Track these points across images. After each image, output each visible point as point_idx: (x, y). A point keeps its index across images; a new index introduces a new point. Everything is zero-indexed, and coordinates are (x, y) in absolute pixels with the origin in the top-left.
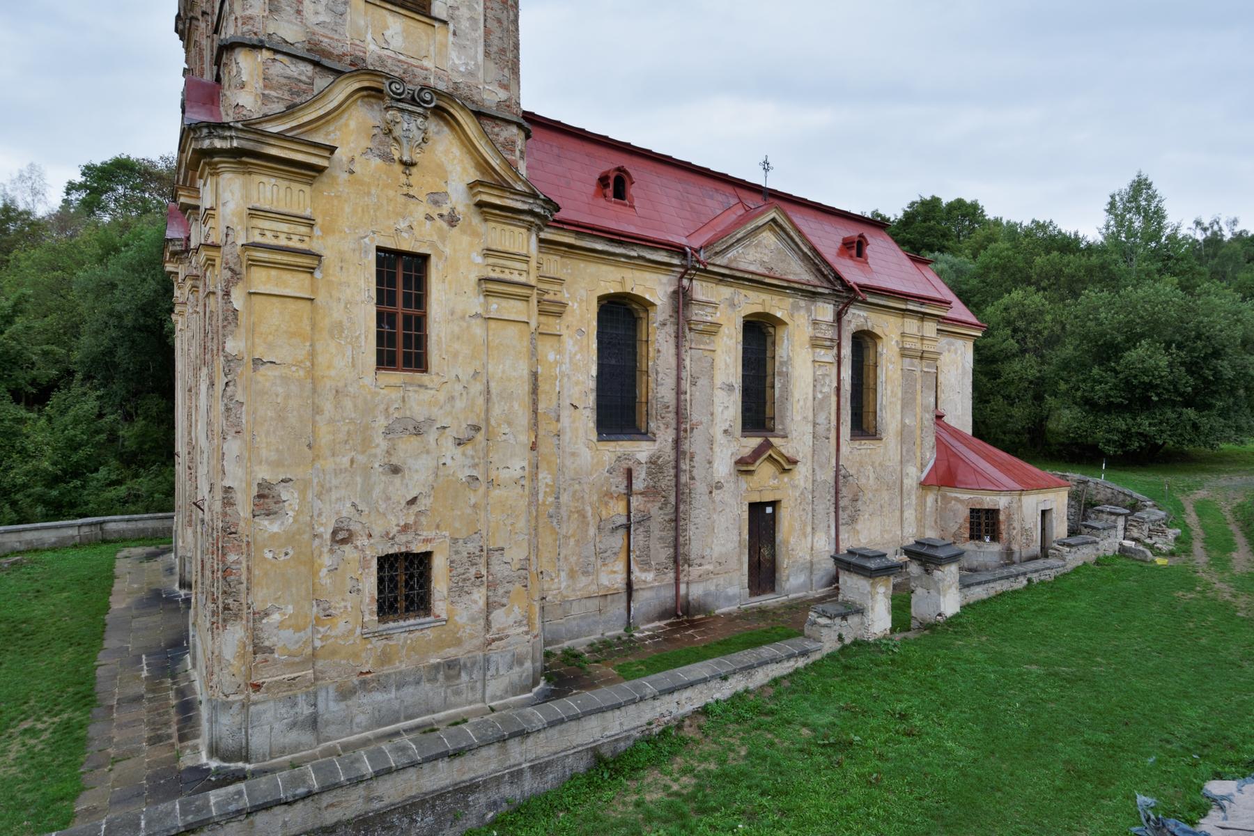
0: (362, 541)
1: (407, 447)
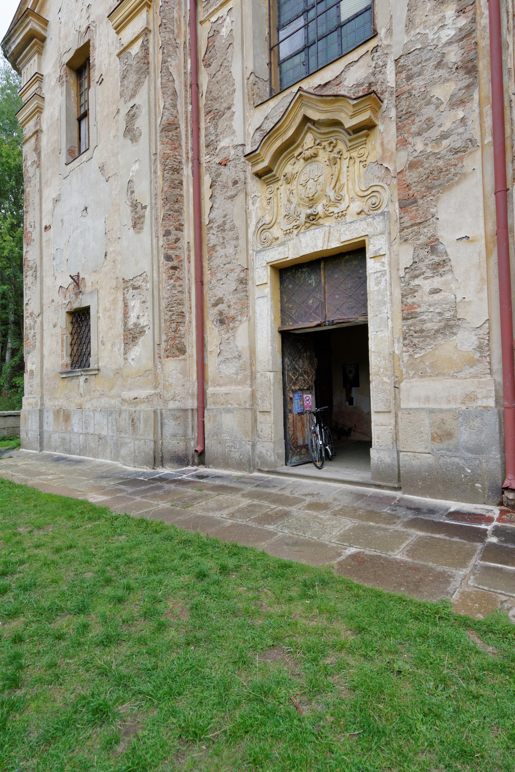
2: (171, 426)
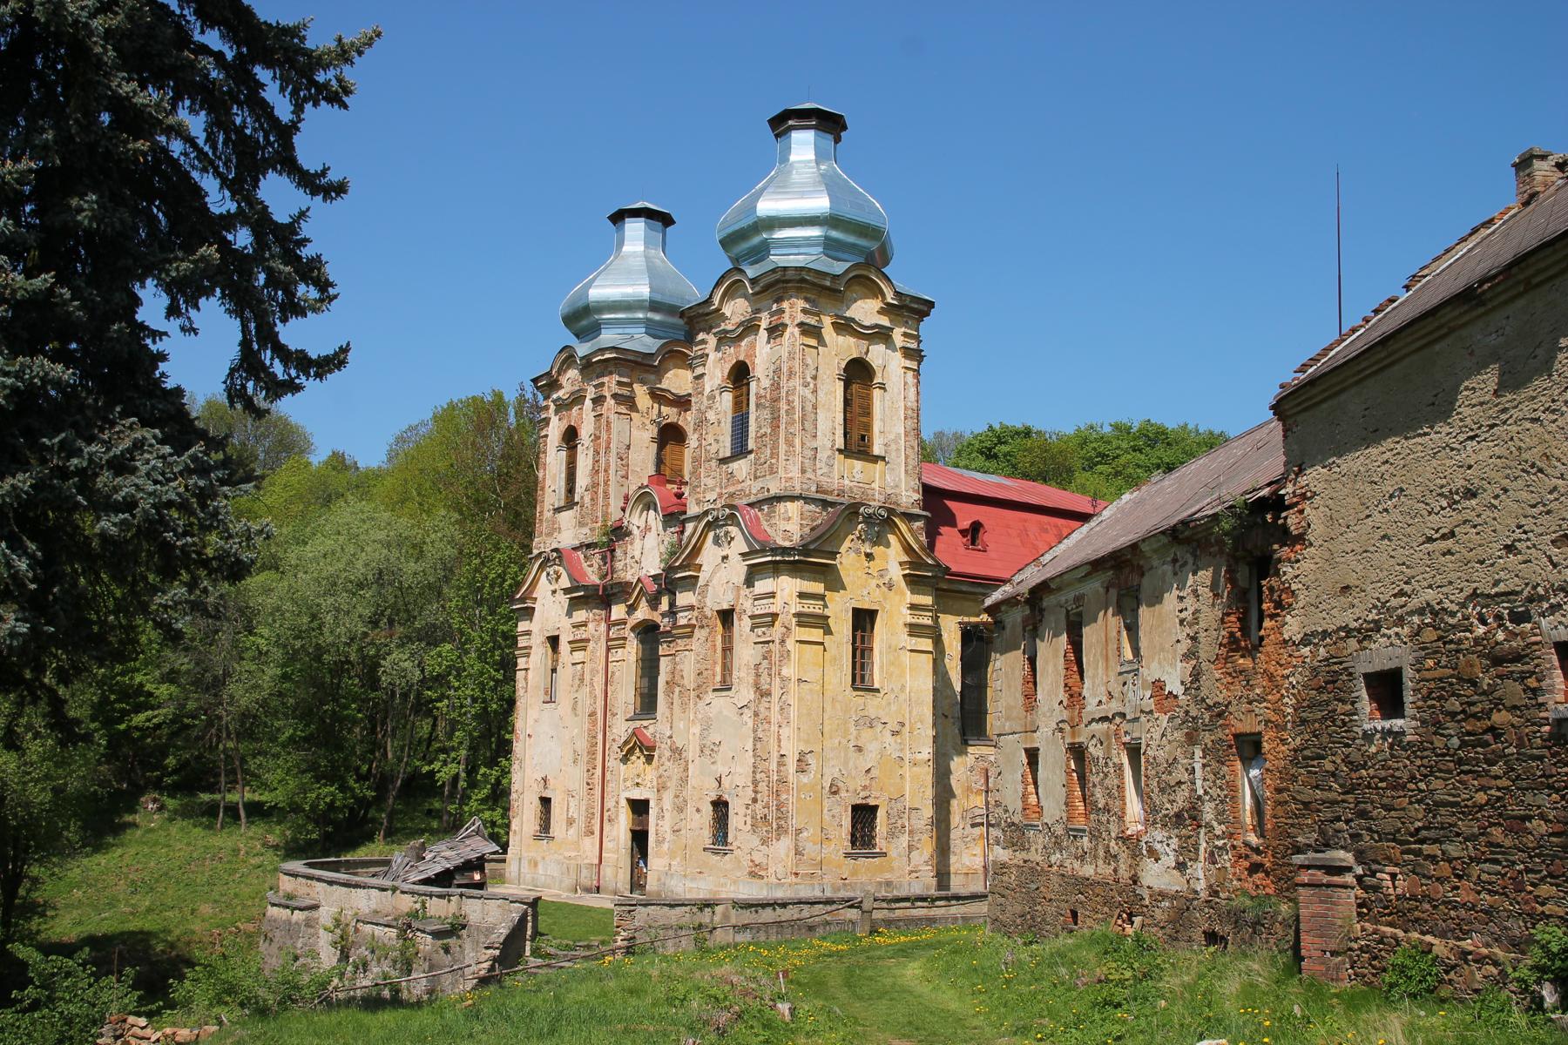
0: (843, 794)
1: (867, 734)
2: (585, 873)
